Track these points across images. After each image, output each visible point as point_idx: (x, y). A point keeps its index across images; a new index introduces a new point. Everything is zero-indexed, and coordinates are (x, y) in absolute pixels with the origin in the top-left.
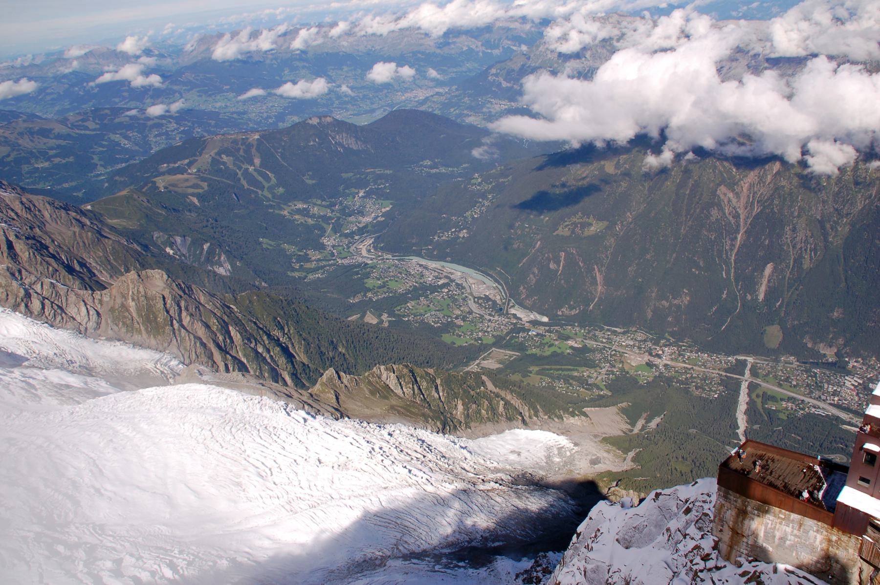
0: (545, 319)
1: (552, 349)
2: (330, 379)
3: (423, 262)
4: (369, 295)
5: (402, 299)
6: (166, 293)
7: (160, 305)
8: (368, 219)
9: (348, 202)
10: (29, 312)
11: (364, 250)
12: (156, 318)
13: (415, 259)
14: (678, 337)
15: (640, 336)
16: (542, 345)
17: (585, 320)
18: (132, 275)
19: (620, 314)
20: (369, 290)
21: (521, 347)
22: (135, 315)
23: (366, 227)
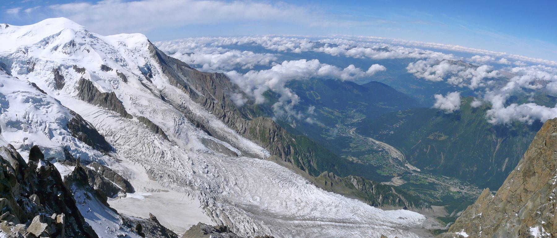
0: (419, 170)
1: (420, 182)
2: (325, 176)
3: (374, 141)
4: (350, 149)
5: (363, 153)
6: (271, 128)
7: (268, 131)
8: (355, 120)
9: (349, 112)
10: (223, 121)
11: (352, 132)
12: (265, 135)
13: (371, 139)
14: (472, 182)
15: (456, 181)
16: (416, 180)
17: (434, 173)
18: (261, 118)
19: (450, 172)
20: (350, 147)
21: (408, 179)
22: (258, 132)
23: (354, 123)
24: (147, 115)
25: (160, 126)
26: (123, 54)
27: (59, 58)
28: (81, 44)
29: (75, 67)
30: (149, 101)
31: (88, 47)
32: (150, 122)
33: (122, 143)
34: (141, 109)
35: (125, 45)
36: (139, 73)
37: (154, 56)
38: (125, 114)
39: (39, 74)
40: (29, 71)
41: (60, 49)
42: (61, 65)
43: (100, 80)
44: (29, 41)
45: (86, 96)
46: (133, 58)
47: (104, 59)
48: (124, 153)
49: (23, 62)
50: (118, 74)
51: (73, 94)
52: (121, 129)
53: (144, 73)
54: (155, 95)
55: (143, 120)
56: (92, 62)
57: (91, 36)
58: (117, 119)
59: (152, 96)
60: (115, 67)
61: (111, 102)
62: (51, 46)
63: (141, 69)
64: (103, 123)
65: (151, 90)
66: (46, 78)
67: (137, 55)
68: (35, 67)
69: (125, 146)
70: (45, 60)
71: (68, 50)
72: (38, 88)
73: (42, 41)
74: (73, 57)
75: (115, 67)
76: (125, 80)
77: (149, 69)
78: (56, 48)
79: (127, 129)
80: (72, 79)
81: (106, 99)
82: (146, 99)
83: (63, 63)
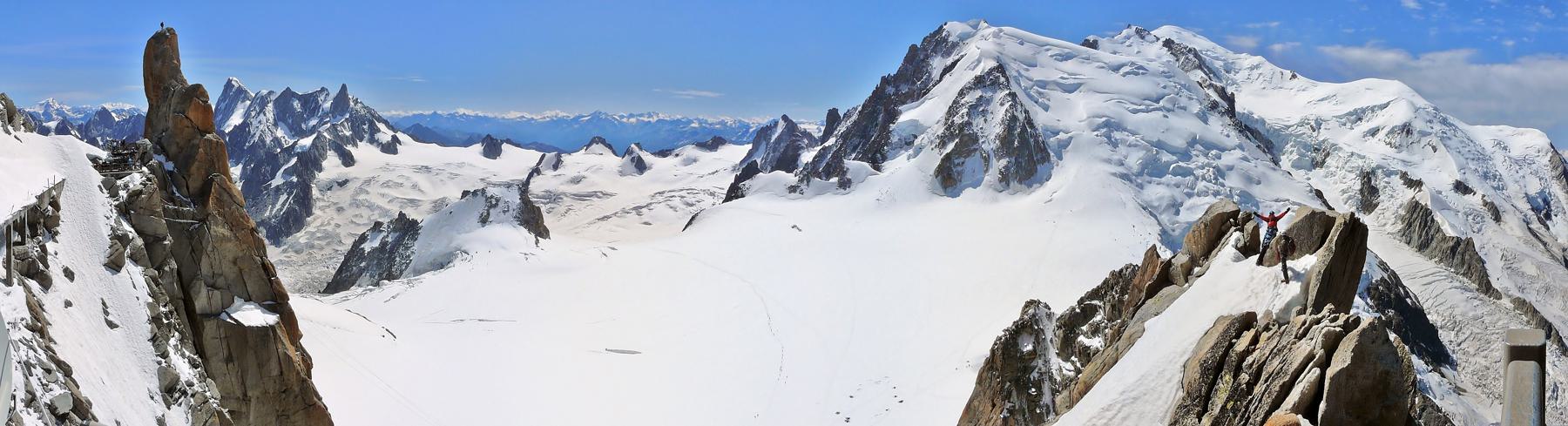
24: (1531, 298)
25: (1556, 324)
26: (1500, 165)
27: (1377, 151)
28: (1424, 134)
29: (1404, 176)
30: (1539, 268)
31: (1435, 141)
32: (1535, 311)
33: (1472, 351)
34: (1520, 281)
35: (1505, 148)
36: (1525, 207)
37: (1558, 178)
38: (1486, 287)
39: (1333, 174)
40: (1316, 164)
41: (1381, 134)
42: (1379, 167)
43: (1449, 209)
44: (1326, 110)
45: (1416, 236)
46: (1517, 176)
47: (1461, 168)
48: (1474, 373)
49: (1306, 146)
50: (1486, 204)
51: (1389, 228)
52: (1475, 318)
53: (1535, 209)
54: (1553, 257)
55: (1521, 304)
56: (1438, 172)
57: (1444, 122)
58: (1469, 294)
59: (1546, 259)
60: (1481, 189)
61: (1462, 257)
62: (1365, 126)
63: (1529, 199)
64: (1440, 300)
65: (1545, 244)
66: (1344, 187)
67: (1526, 170)
68: (1328, 160)
69: (1477, 359)
70: (1350, 150)
71: (1397, 140)
72: (1325, 202)
73: (1350, 114)
74: (1404, 155)
75: (1481, 189)
76: (1497, 218)
77: (1546, 202)
78: (1374, 132)
79: (1487, 319)
80: (1395, 197)
81: (1453, 250)
82: (1533, 262)
83: (1382, 163)
